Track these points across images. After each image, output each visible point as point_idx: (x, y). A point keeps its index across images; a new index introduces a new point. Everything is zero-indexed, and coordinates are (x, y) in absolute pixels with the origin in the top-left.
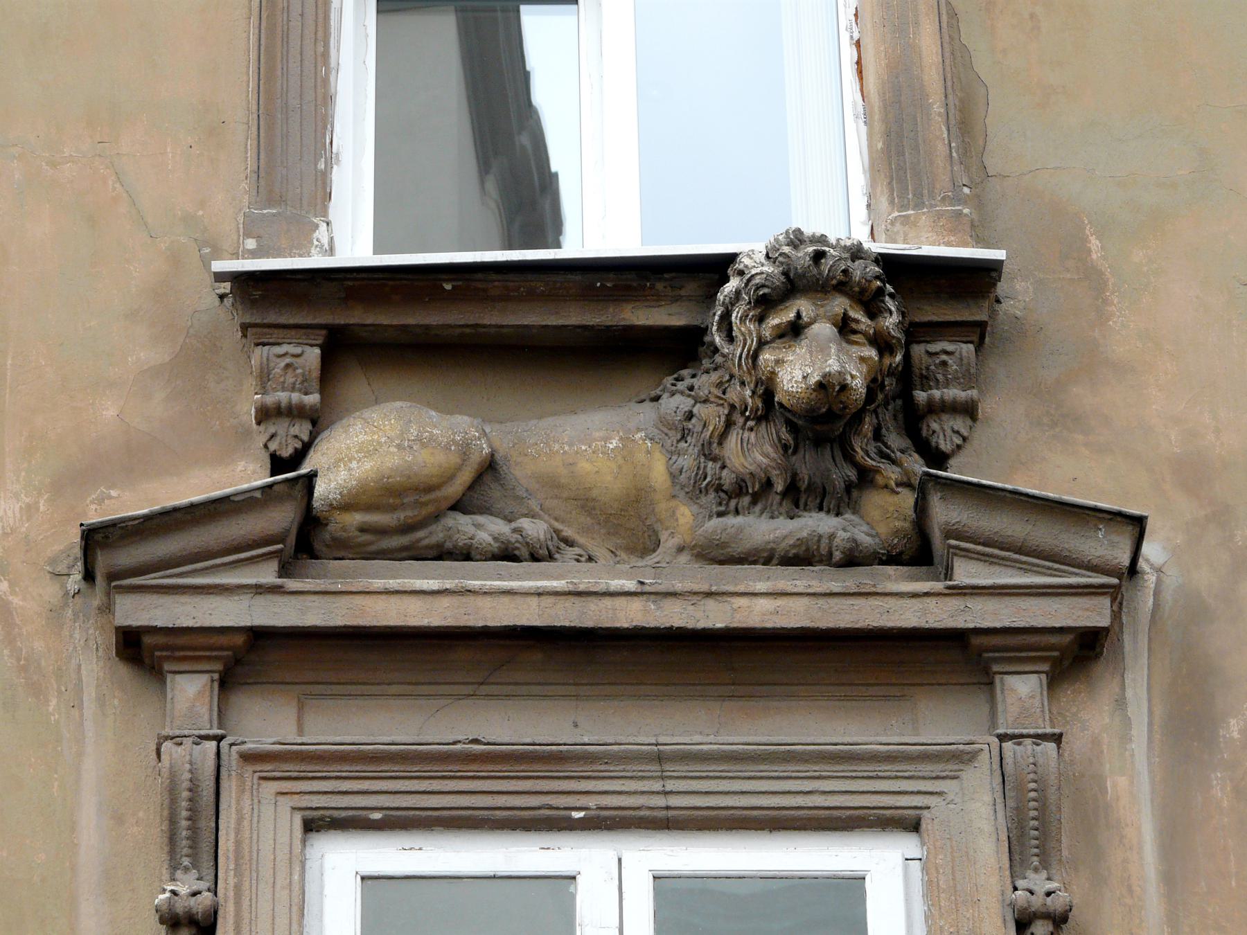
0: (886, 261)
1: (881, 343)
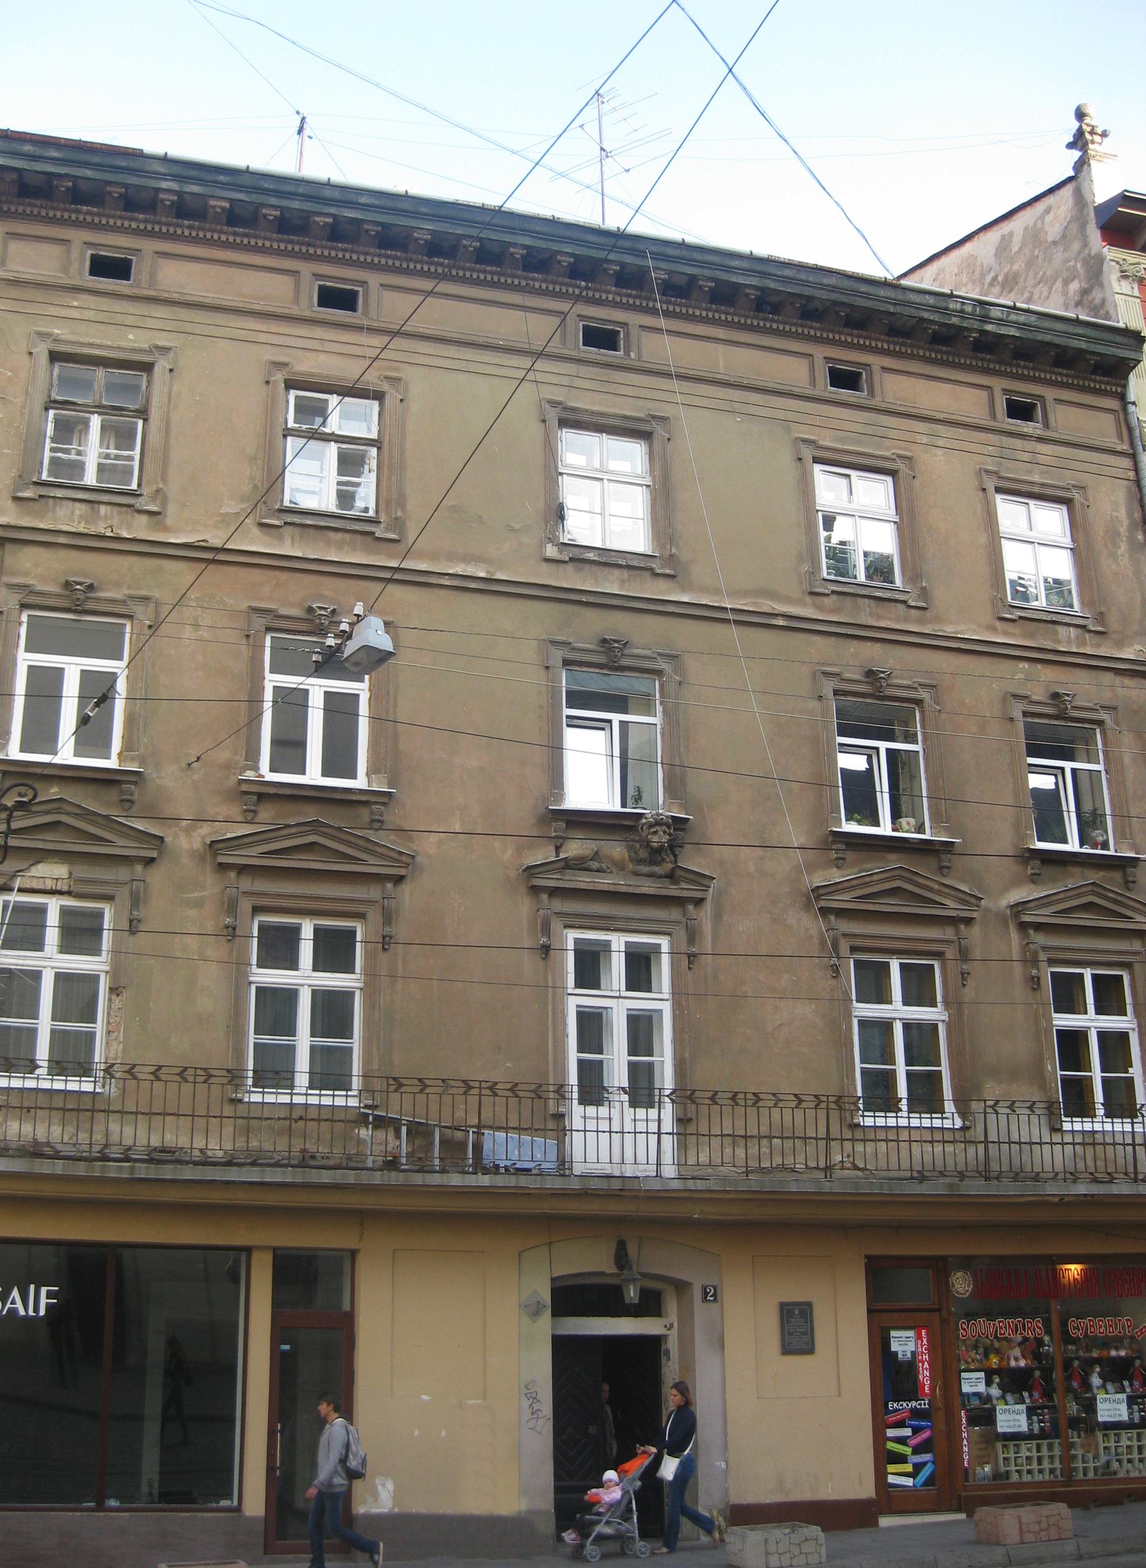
0: (673, 817)
1: (670, 835)
